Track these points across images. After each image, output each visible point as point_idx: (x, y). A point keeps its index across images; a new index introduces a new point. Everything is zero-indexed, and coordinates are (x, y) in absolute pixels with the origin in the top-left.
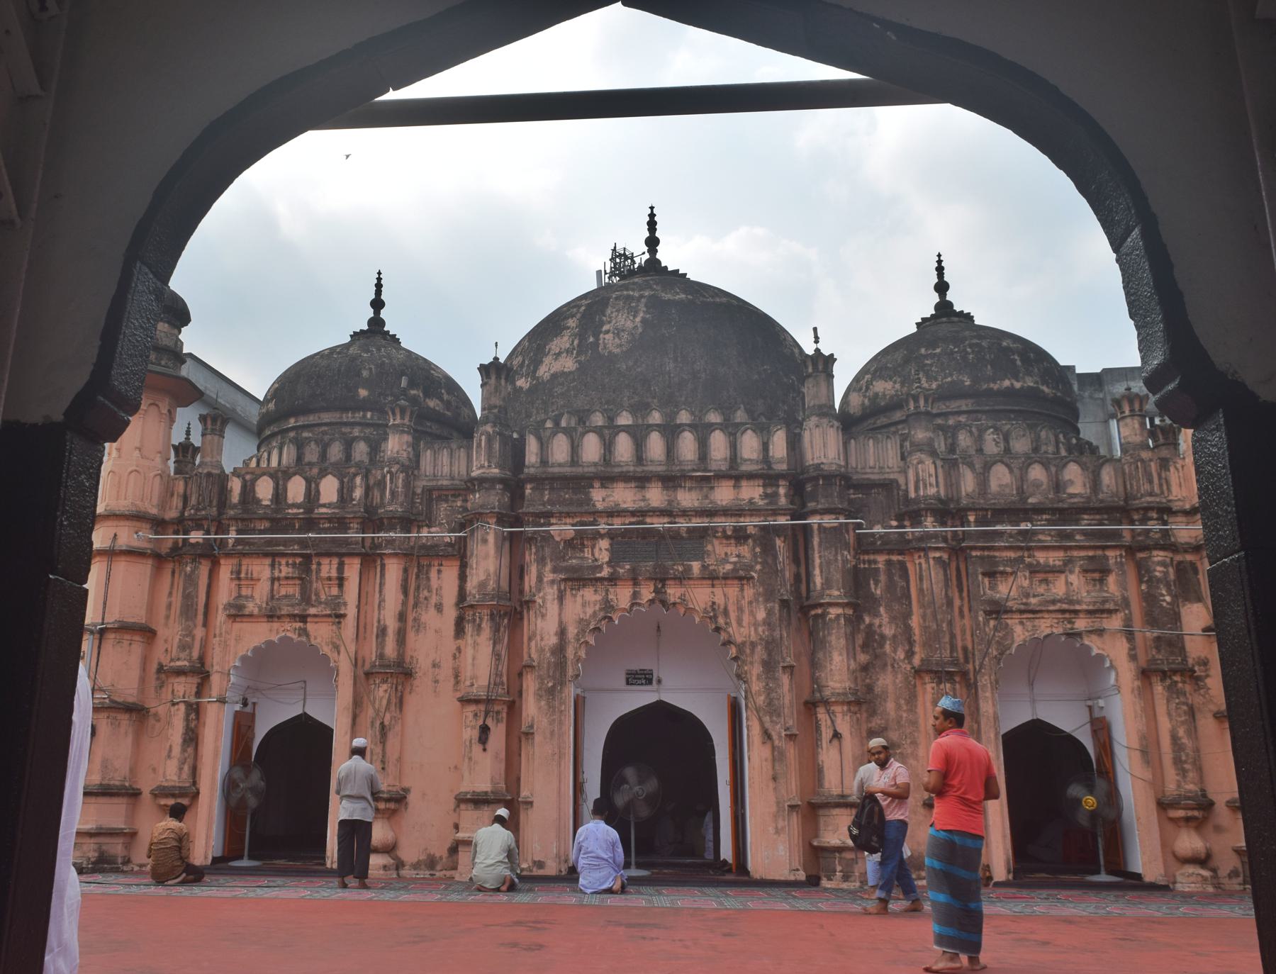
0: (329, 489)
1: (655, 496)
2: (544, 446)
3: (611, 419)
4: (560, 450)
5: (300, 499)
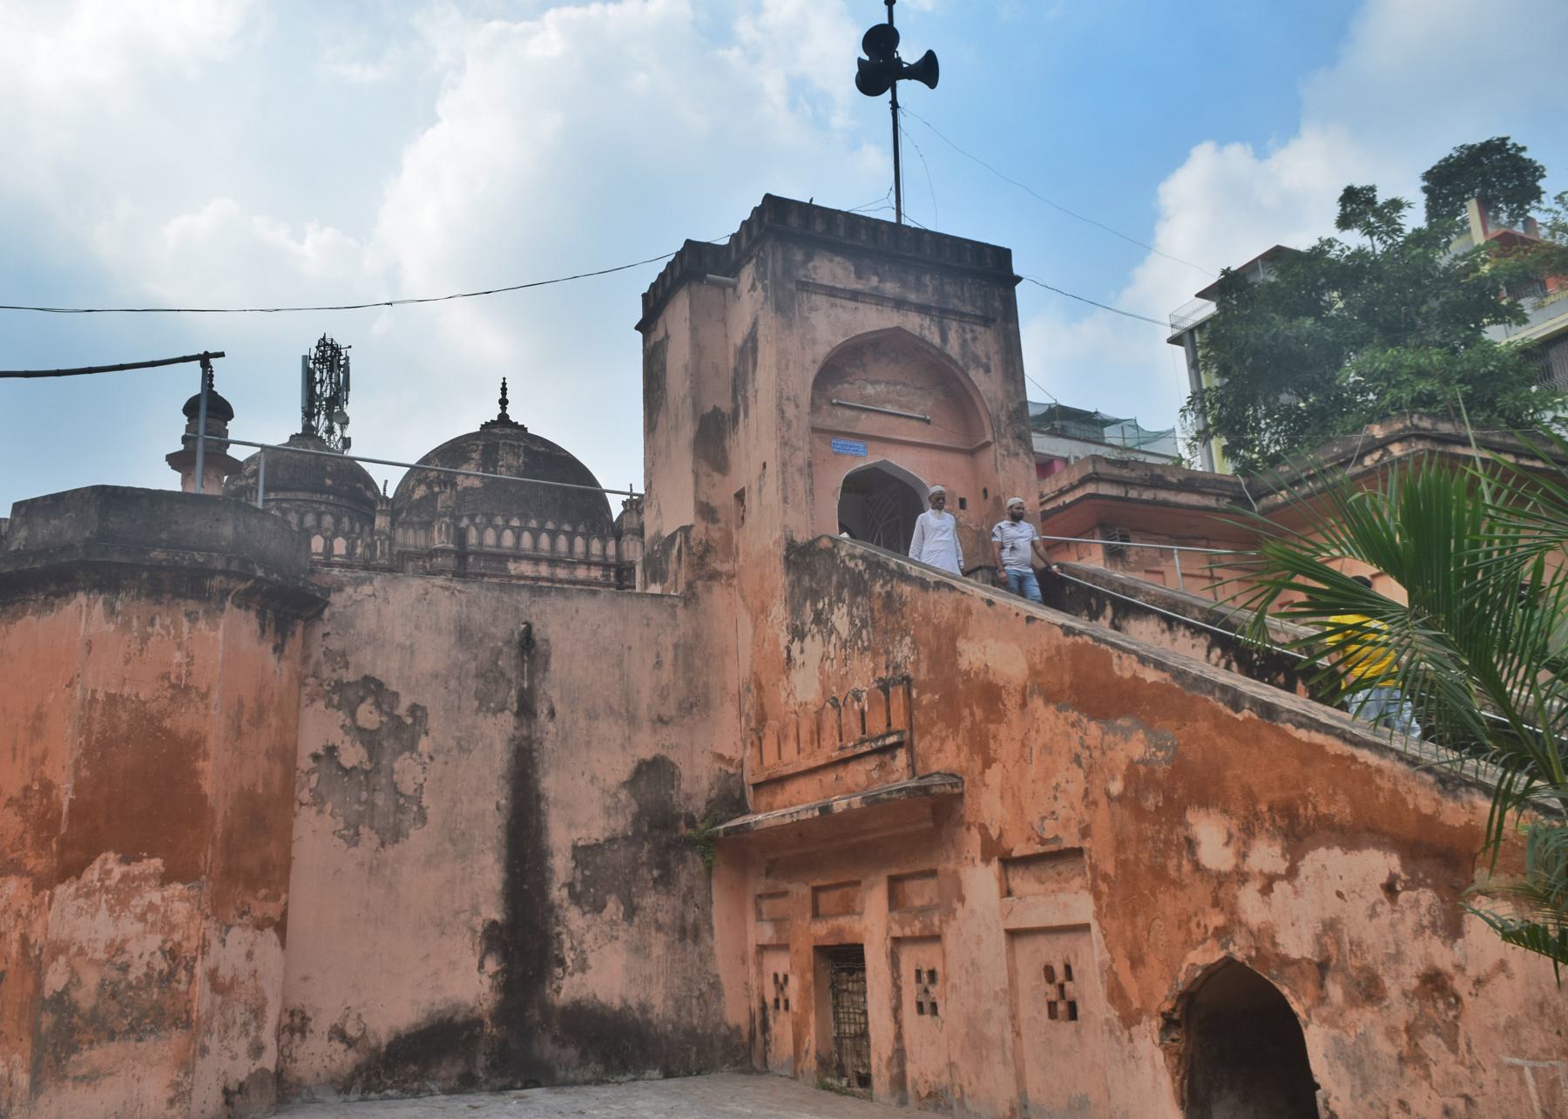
0: (340, 546)
1: (544, 570)
2: (481, 534)
3: (507, 522)
4: (490, 537)
5: (320, 550)
